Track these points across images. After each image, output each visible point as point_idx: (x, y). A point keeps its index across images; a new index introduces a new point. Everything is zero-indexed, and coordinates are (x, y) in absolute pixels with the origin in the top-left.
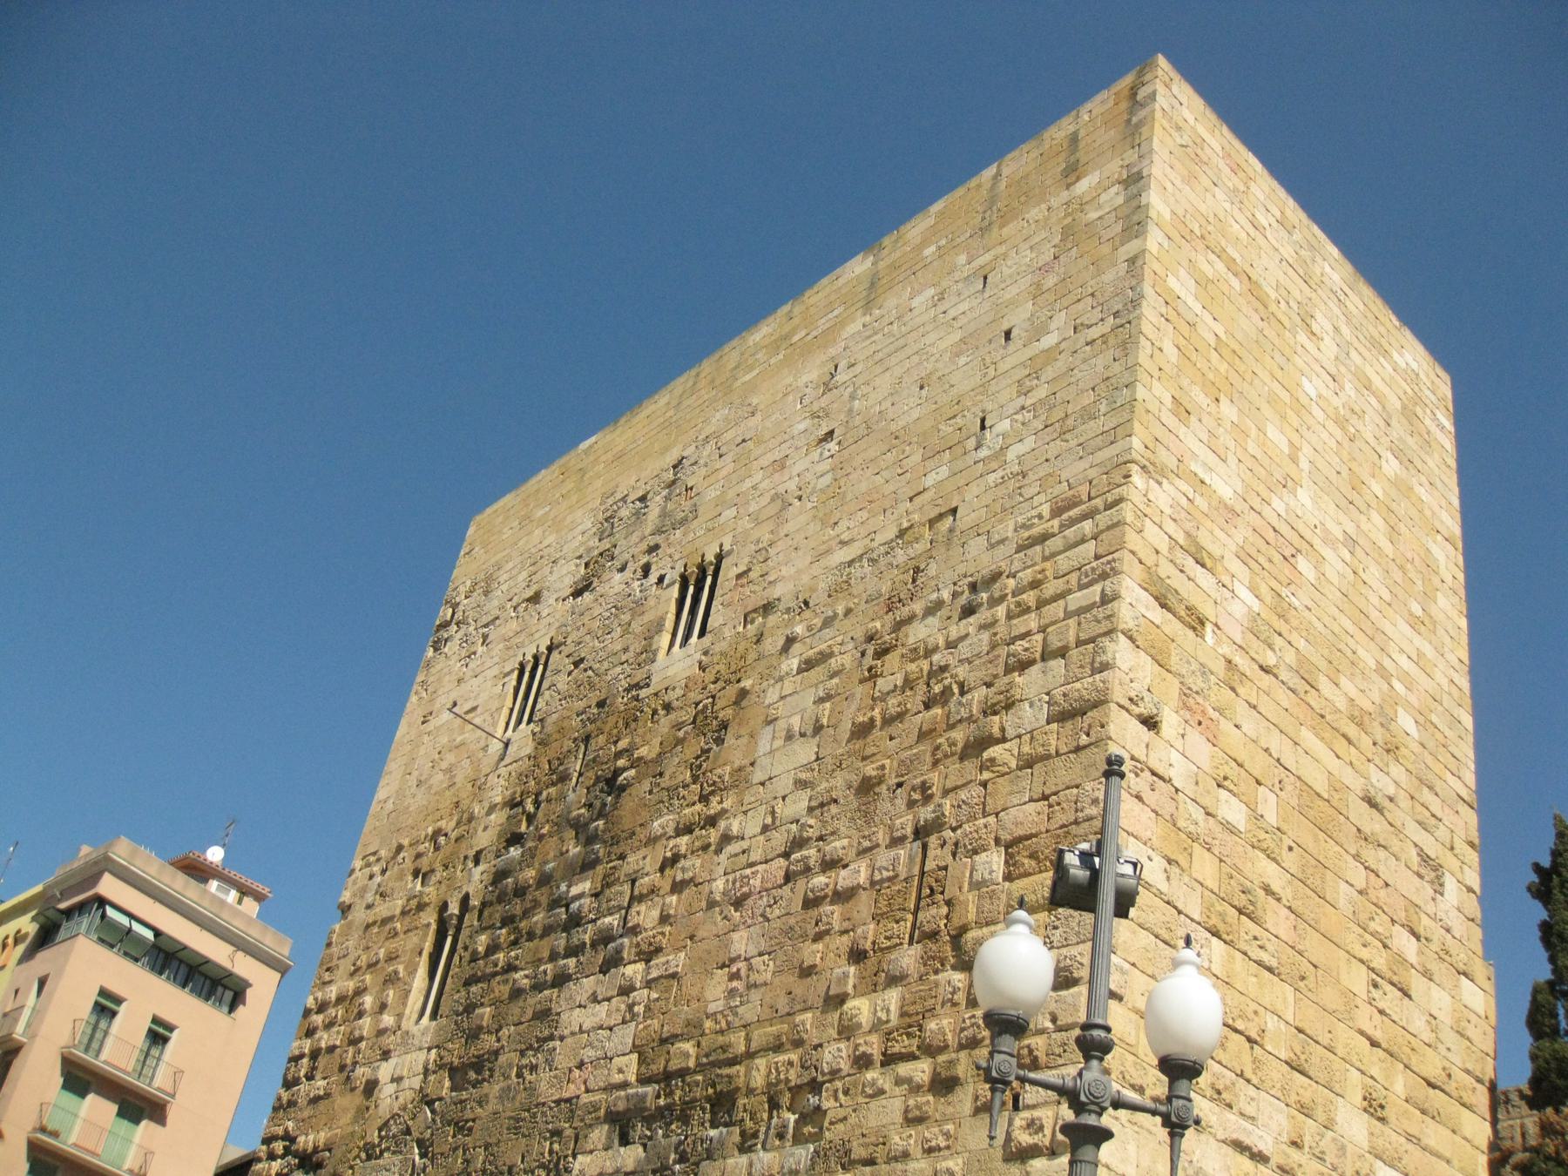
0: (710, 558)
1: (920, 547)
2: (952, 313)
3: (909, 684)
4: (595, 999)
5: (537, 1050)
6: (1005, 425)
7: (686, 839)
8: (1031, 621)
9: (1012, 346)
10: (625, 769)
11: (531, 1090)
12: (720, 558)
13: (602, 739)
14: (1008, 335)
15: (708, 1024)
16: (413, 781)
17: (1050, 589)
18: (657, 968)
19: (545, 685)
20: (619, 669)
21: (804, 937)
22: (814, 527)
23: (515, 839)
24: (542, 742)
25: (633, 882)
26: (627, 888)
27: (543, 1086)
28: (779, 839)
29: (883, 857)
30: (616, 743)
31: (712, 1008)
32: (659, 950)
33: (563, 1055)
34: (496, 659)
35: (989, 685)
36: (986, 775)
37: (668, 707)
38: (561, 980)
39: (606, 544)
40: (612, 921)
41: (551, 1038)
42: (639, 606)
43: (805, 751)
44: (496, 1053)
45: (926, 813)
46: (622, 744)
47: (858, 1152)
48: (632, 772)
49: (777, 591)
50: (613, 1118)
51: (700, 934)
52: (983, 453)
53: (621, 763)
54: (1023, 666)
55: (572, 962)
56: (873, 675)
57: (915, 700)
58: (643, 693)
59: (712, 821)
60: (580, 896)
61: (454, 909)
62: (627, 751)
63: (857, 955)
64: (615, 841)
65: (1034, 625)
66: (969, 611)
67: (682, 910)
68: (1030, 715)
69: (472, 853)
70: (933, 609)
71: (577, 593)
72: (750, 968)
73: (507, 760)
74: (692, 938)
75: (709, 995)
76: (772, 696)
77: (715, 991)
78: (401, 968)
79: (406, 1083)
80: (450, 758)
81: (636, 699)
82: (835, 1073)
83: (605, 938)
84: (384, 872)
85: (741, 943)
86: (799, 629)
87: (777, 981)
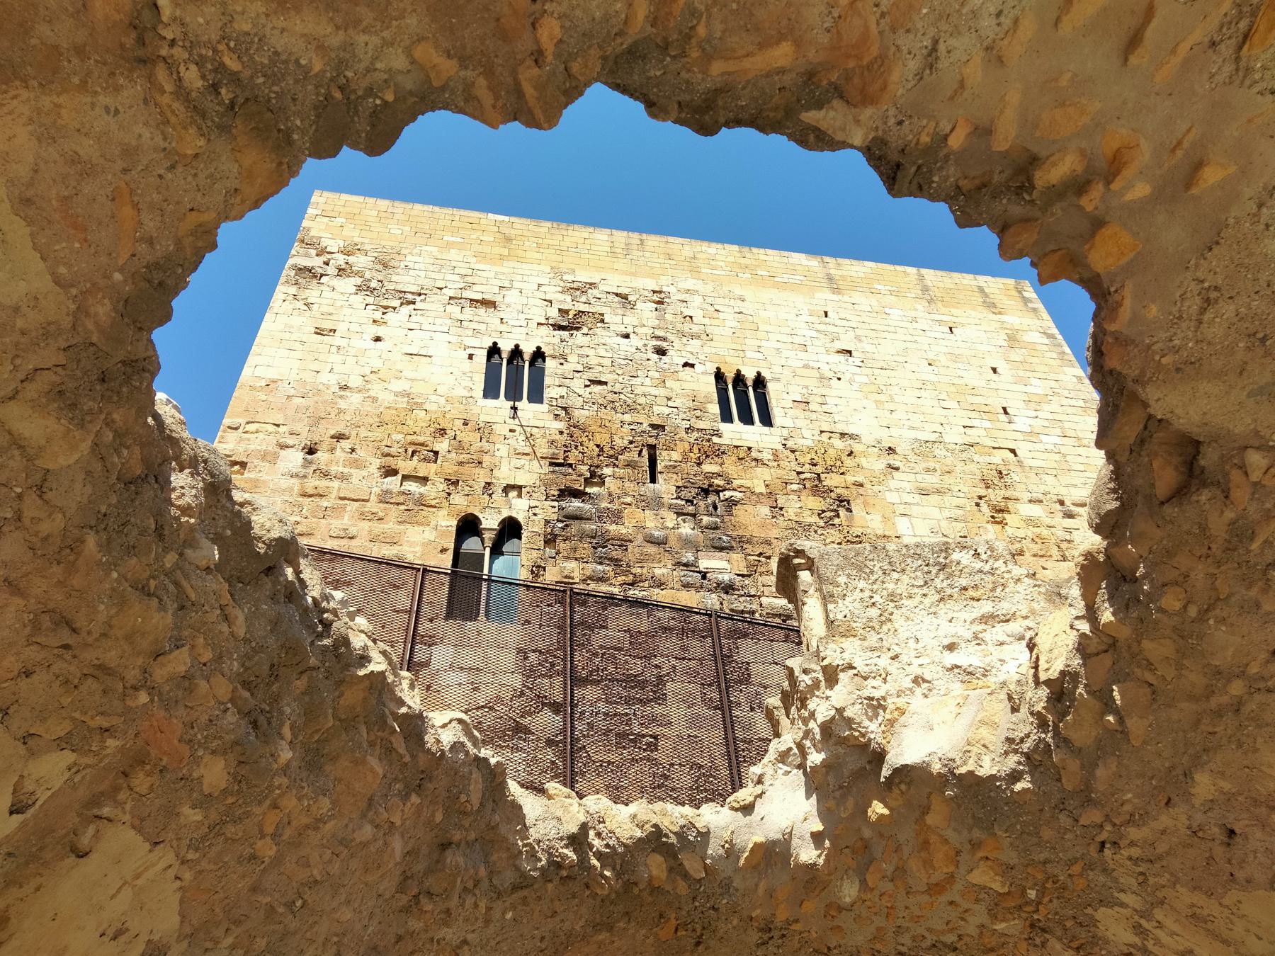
0: (750, 375)
13: (676, 456)
19: (547, 381)
20: (667, 411)
23: (569, 492)
30: (699, 464)
46: (709, 467)
53: (718, 482)
58: (715, 439)
60: (720, 571)
69: (505, 482)
80: (397, 386)
81: (709, 440)
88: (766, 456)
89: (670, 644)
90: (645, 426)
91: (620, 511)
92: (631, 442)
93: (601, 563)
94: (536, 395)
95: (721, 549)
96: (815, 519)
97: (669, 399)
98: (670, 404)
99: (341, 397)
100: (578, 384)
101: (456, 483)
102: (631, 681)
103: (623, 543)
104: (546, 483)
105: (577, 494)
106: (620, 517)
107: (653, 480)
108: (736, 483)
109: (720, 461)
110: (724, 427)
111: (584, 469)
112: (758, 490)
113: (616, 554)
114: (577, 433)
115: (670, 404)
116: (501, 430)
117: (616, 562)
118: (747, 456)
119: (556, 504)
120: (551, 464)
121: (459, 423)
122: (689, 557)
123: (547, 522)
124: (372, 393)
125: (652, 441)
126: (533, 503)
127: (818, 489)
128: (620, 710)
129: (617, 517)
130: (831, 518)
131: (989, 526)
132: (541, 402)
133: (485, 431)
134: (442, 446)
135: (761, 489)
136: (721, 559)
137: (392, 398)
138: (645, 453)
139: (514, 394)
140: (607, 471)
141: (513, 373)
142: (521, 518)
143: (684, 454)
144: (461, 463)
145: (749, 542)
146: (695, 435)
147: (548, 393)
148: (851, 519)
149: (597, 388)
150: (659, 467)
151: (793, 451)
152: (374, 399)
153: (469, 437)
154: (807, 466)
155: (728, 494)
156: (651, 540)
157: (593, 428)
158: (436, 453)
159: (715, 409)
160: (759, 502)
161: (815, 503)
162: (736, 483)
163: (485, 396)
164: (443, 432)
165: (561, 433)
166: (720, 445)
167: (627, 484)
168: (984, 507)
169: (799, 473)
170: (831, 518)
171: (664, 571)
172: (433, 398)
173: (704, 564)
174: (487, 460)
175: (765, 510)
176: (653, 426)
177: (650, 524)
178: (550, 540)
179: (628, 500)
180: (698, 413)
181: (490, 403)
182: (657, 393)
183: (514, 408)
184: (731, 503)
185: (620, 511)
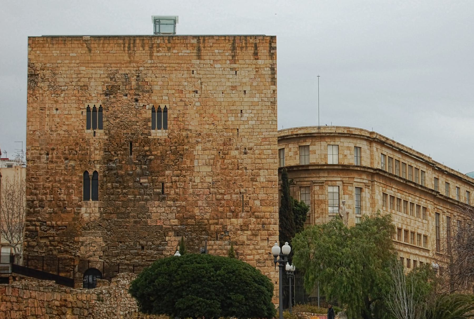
1: (231, 134)
2: (228, 76)
3: (232, 163)
4: (159, 206)
5: (143, 214)
6: (247, 115)
7: (178, 178)
8: (259, 161)
9: (247, 95)
10: (150, 155)
11: (146, 223)
12: (166, 108)
14: (245, 91)
15: (196, 217)
16: (47, 128)
17: (263, 157)
18: (178, 204)
19: (104, 119)
21: (218, 206)
22: (197, 115)
24: (111, 138)
25: (163, 184)
26: (161, 184)
27: (149, 222)
28: (205, 185)
29: (234, 196)
30: (144, 147)
31: (197, 214)
32: (177, 200)
33: (154, 216)
34: (74, 101)
35: (252, 170)
36: (254, 187)
37: (159, 143)
38: (147, 200)
39: (113, 83)
40: (160, 191)
41: (146, 212)
42: (138, 112)
43: (209, 169)
44: (129, 213)
45: (242, 190)
46: (147, 148)
47: (239, 243)
48: (153, 157)
49: (190, 127)
50: (175, 231)
51: (188, 199)
52: (243, 119)
53: (148, 153)
54: (260, 169)
55: (149, 197)
56: (223, 159)
57: (236, 167)
58: (149, 137)
59: (185, 176)
60: (145, 183)
61: (91, 173)
62: (150, 150)
63: (231, 211)
64: (151, 173)
65: (260, 162)
66: (245, 153)
67: (181, 193)
68: (262, 179)
69: (93, 160)
70: (237, 149)
71: (106, 95)
72: (205, 209)
73: (96, 137)
74: (186, 199)
75: (195, 212)
76: (195, 153)
77: (197, 211)
78: (74, 185)
79: (93, 215)
80: (65, 128)
82: (231, 230)
83: (158, 194)
84: (48, 154)
85: (200, 203)
86: (199, 140)
87: (213, 212)
88: (163, 142)
89: (131, 204)
90: (130, 135)
91: (122, 166)
92: (126, 141)
93: (116, 182)
94: (101, 128)
95: (146, 176)
96: (172, 163)
97: (137, 122)
98: (137, 124)
99: (51, 134)
100: (112, 121)
101: (82, 161)
102: (123, 213)
103: (122, 176)
104: (104, 158)
105: (111, 161)
106: (122, 168)
107: (131, 154)
108: (153, 153)
109: (149, 145)
110: (153, 131)
111: (113, 152)
112: (158, 155)
113: (121, 180)
114: (111, 139)
115: (137, 124)
116: (92, 141)
117: (120, 182)
118: (157, 141)
119: (106, 165)
120: (105, 152)
121: (81, 140)
122: (138, 179)
123: (104, 171)
124: (59, 132)
125: (131, 140)
126: (101, 166)
127: (175, 153)
128: (120, 220)
129: (121, 168)
130: (177, 162)
131: (220, 160)
132: (102, 129)
133: (87, 142)
134: (78, 149)
135: (159, 154)
136: (145, 179)
137: (64, 133)
138: (129, 145)
139: (94, 128)
140: (119, 152)
141: (94, 117)
142: (98, 171)
143: (140, 144)
144: (83, 155)
145: (153, 172)
146: (144, 136)
147: (105, 124)
148: (182, 162)
149: (117, 120)
150: (133, 149)
151: (170, 139)
152: (59, 134)
153: (84, 145)
154: (174, 144)
155: (150, 157)
156: (129, 174)
157: (116, 137)
158: (76, 151)
159: (150, 124)
160: (158, 159)
161: (172, 157)
162: (153, 153)
163: (87, 129)
164: (77, 144)
165: (107, 140)
166: (149, 139)
167: (124, 156)
168: (221, 153)
169: (171, 147)
170: (177, 162)
171: (132, 184)
172: (74, 131)
173: (142, 181)
174: (89, 152)
175: (159, 162)
176: (132, 134)
177: (129, 169)
178: (105, 176)
179: (124, 162)
180: (145, 127)
181: (89, 131)
182: (134, 120)
183: (95, 132)
184: (151, 160)
185: (122, 166)
